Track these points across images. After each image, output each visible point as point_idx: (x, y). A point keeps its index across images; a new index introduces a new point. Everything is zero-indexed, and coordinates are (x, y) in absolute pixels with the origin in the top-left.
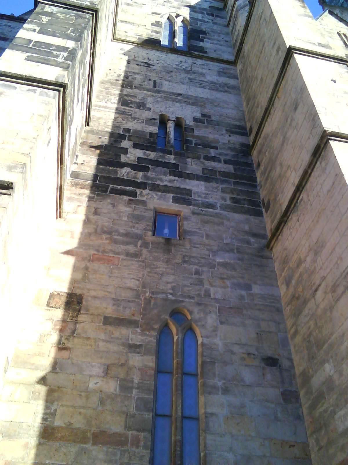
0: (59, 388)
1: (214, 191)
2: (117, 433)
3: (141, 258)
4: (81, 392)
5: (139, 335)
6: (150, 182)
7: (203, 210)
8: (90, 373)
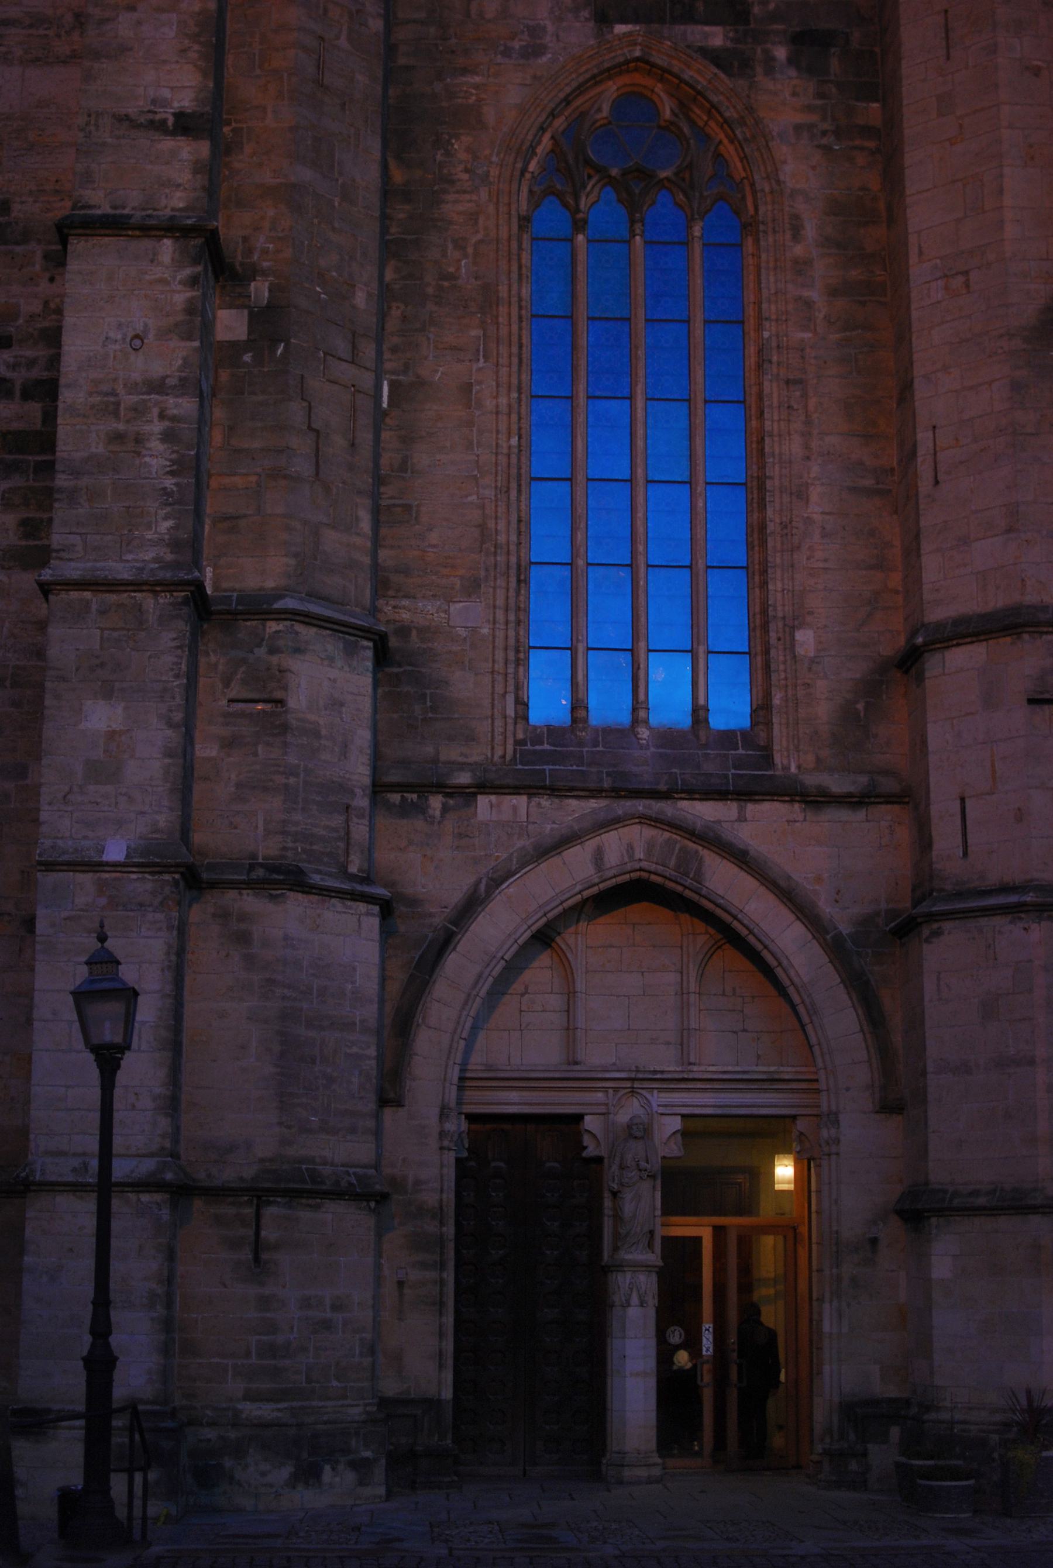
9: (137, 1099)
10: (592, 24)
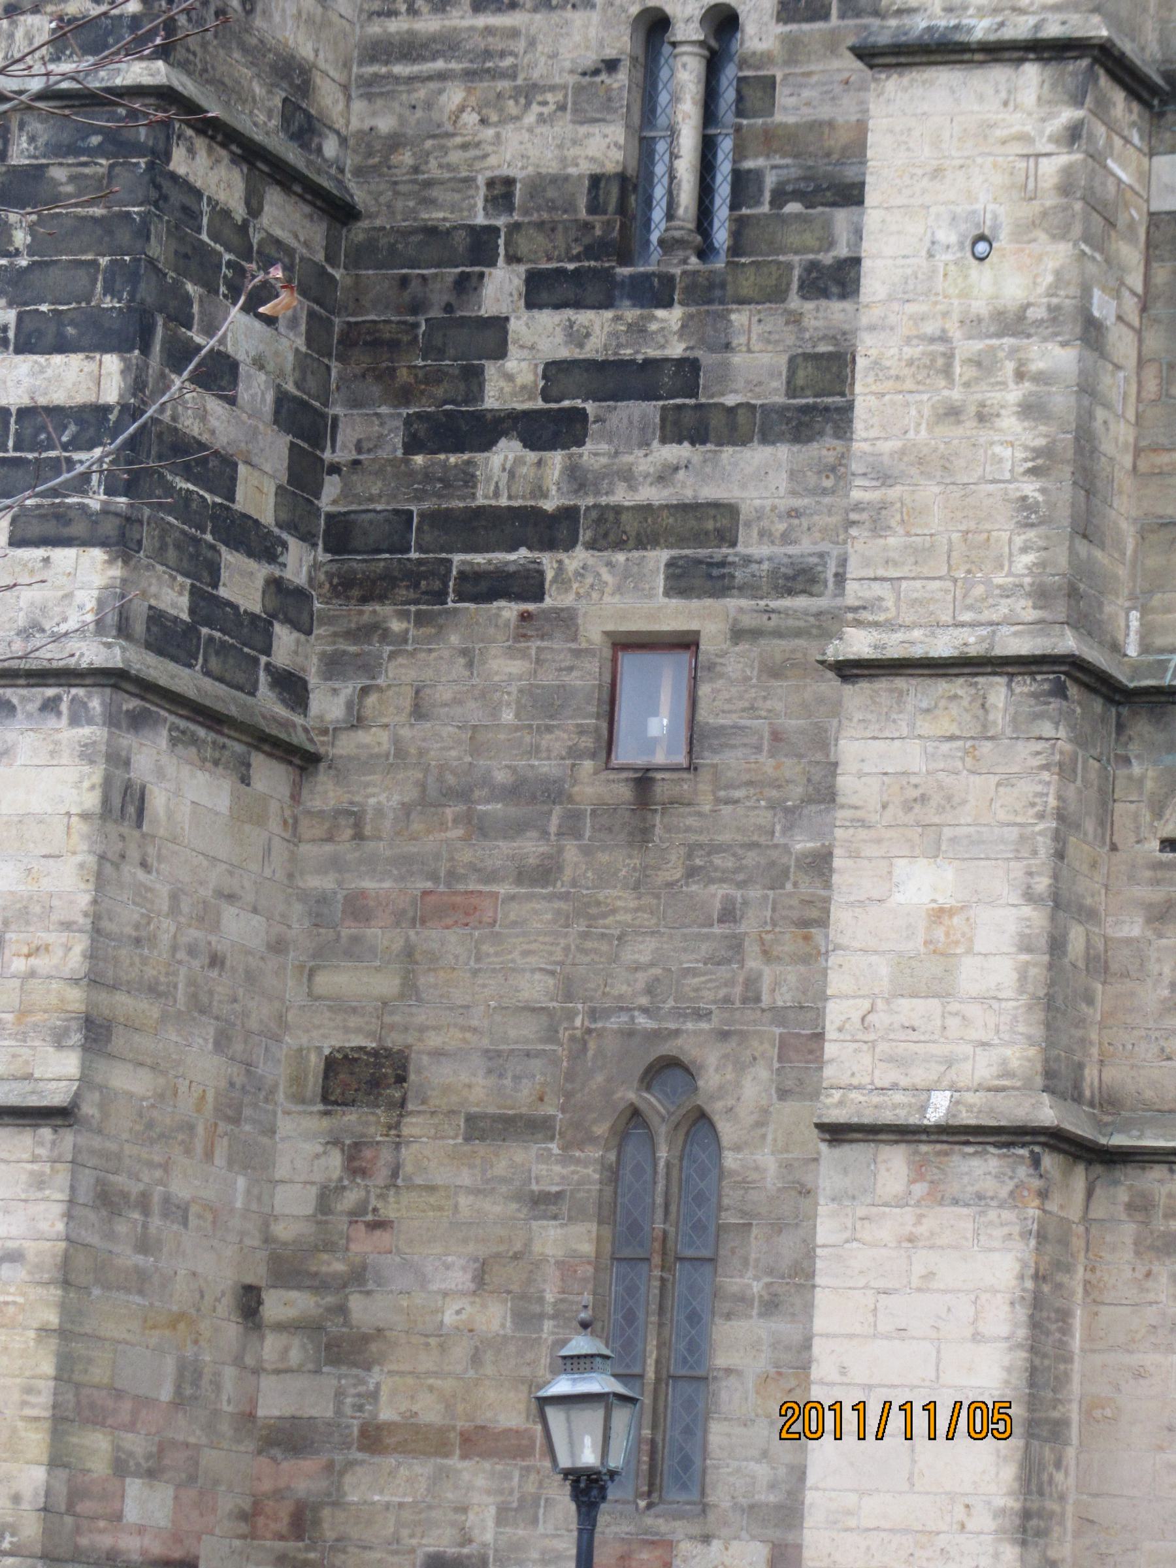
0: (379, 1330)
1: (824, 492)
2: (510, 1430)
3: (559, 884)
4: (426, 1336)
5: (557, 1162)
6: (590, 501)
7: (773, 611)
8: (443, 1286)
9: (969, 1515)
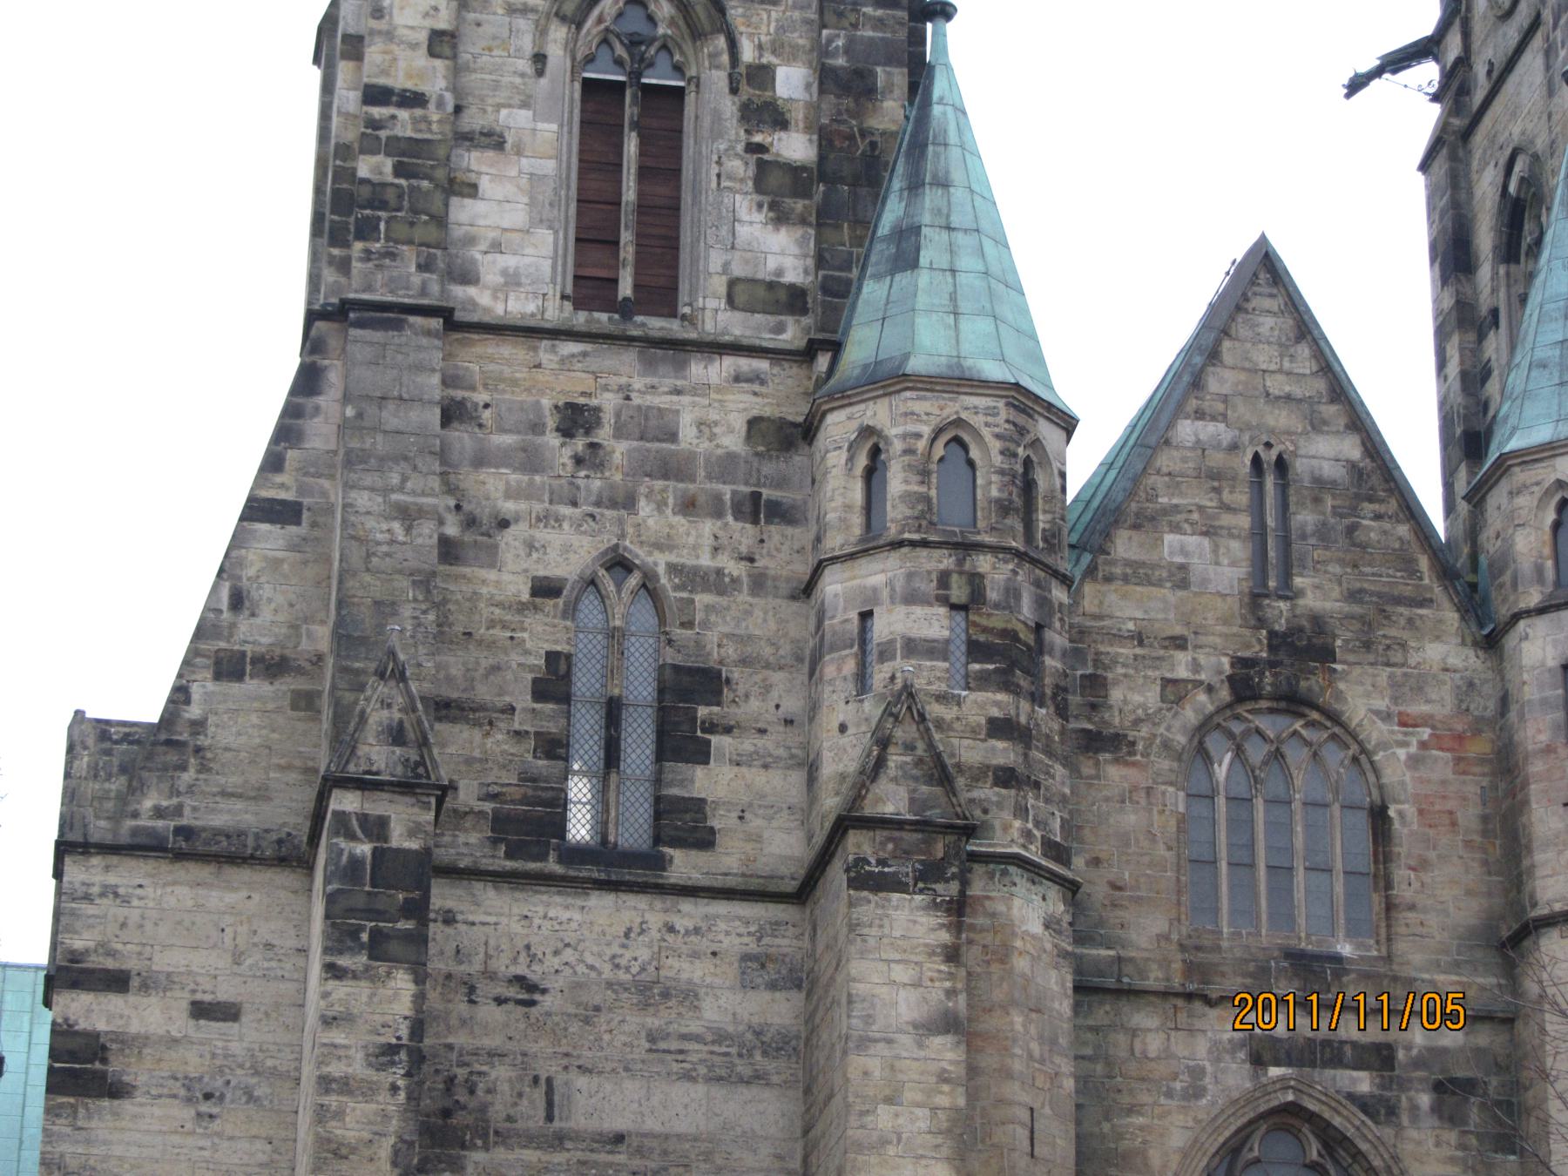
10: (1248, 1066)
